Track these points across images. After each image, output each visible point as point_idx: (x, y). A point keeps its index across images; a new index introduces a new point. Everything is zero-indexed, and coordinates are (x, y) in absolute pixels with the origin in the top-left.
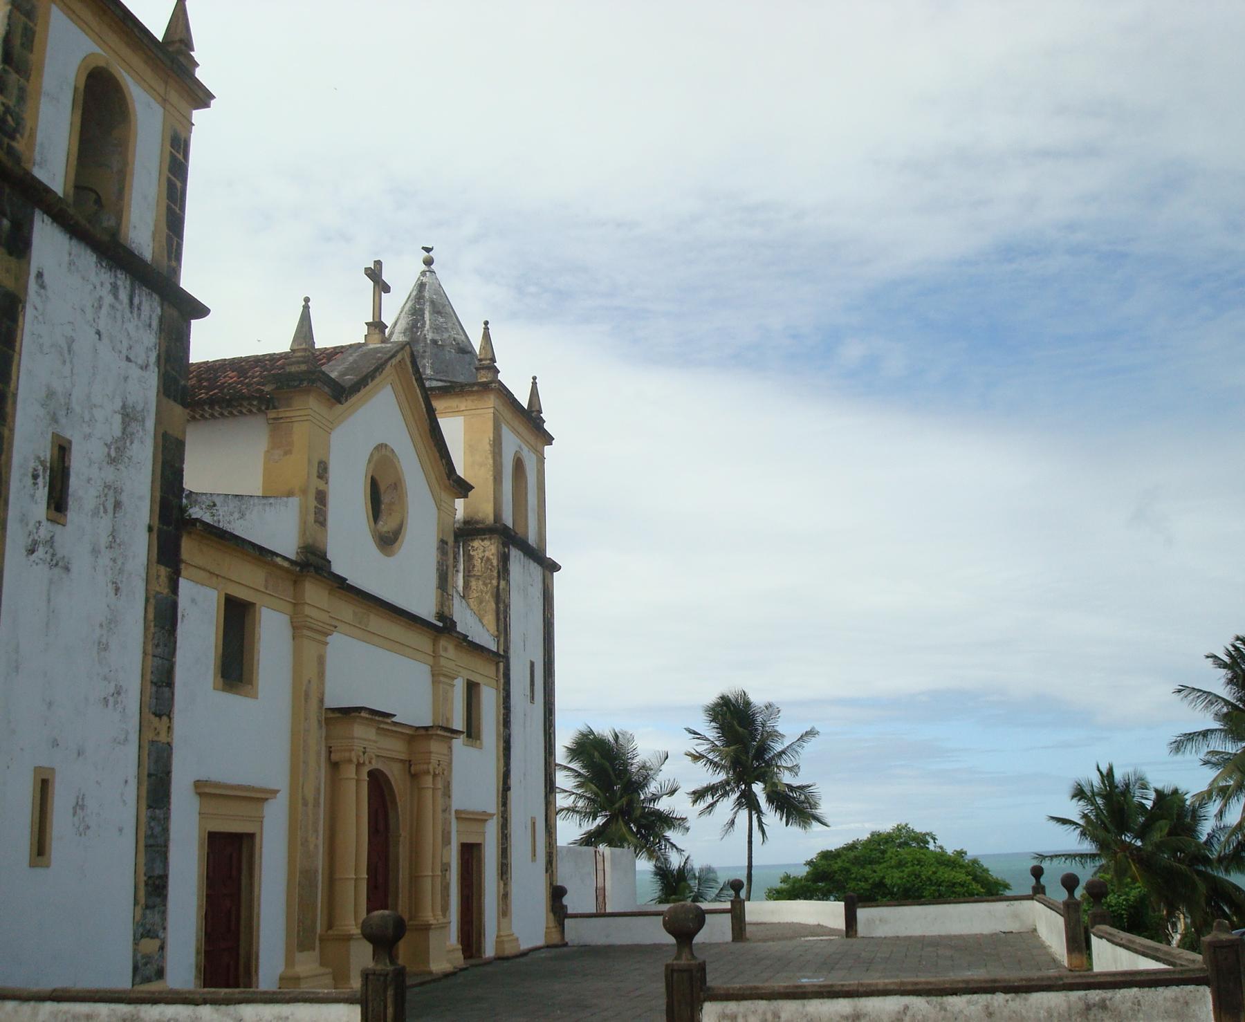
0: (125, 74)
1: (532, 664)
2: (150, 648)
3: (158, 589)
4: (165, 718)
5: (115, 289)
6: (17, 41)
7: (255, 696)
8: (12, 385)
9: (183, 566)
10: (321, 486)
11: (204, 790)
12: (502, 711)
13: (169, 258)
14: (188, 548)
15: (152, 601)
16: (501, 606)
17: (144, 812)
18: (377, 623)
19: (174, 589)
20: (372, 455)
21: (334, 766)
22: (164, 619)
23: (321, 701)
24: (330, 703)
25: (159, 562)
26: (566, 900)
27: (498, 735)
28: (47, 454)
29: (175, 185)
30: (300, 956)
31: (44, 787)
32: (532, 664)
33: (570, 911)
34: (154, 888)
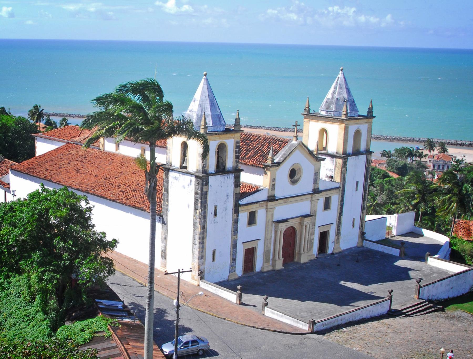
1: (357, 182)
5: (224, 178)
10: (273, 183)
12: (340, 199)
14: (240, 209)
17: (232, 250)
18: (290, 199)
19: (238, 216)
21: (276, 232)
22: (236, 222)
24: (275, 220)
26: (365, 235)
27: (338, 205)
28: (213, 209)
30: (265, 264)
31: (214, 252)
32: (357, 182)
33: (366, 238)
34: (234, 260)
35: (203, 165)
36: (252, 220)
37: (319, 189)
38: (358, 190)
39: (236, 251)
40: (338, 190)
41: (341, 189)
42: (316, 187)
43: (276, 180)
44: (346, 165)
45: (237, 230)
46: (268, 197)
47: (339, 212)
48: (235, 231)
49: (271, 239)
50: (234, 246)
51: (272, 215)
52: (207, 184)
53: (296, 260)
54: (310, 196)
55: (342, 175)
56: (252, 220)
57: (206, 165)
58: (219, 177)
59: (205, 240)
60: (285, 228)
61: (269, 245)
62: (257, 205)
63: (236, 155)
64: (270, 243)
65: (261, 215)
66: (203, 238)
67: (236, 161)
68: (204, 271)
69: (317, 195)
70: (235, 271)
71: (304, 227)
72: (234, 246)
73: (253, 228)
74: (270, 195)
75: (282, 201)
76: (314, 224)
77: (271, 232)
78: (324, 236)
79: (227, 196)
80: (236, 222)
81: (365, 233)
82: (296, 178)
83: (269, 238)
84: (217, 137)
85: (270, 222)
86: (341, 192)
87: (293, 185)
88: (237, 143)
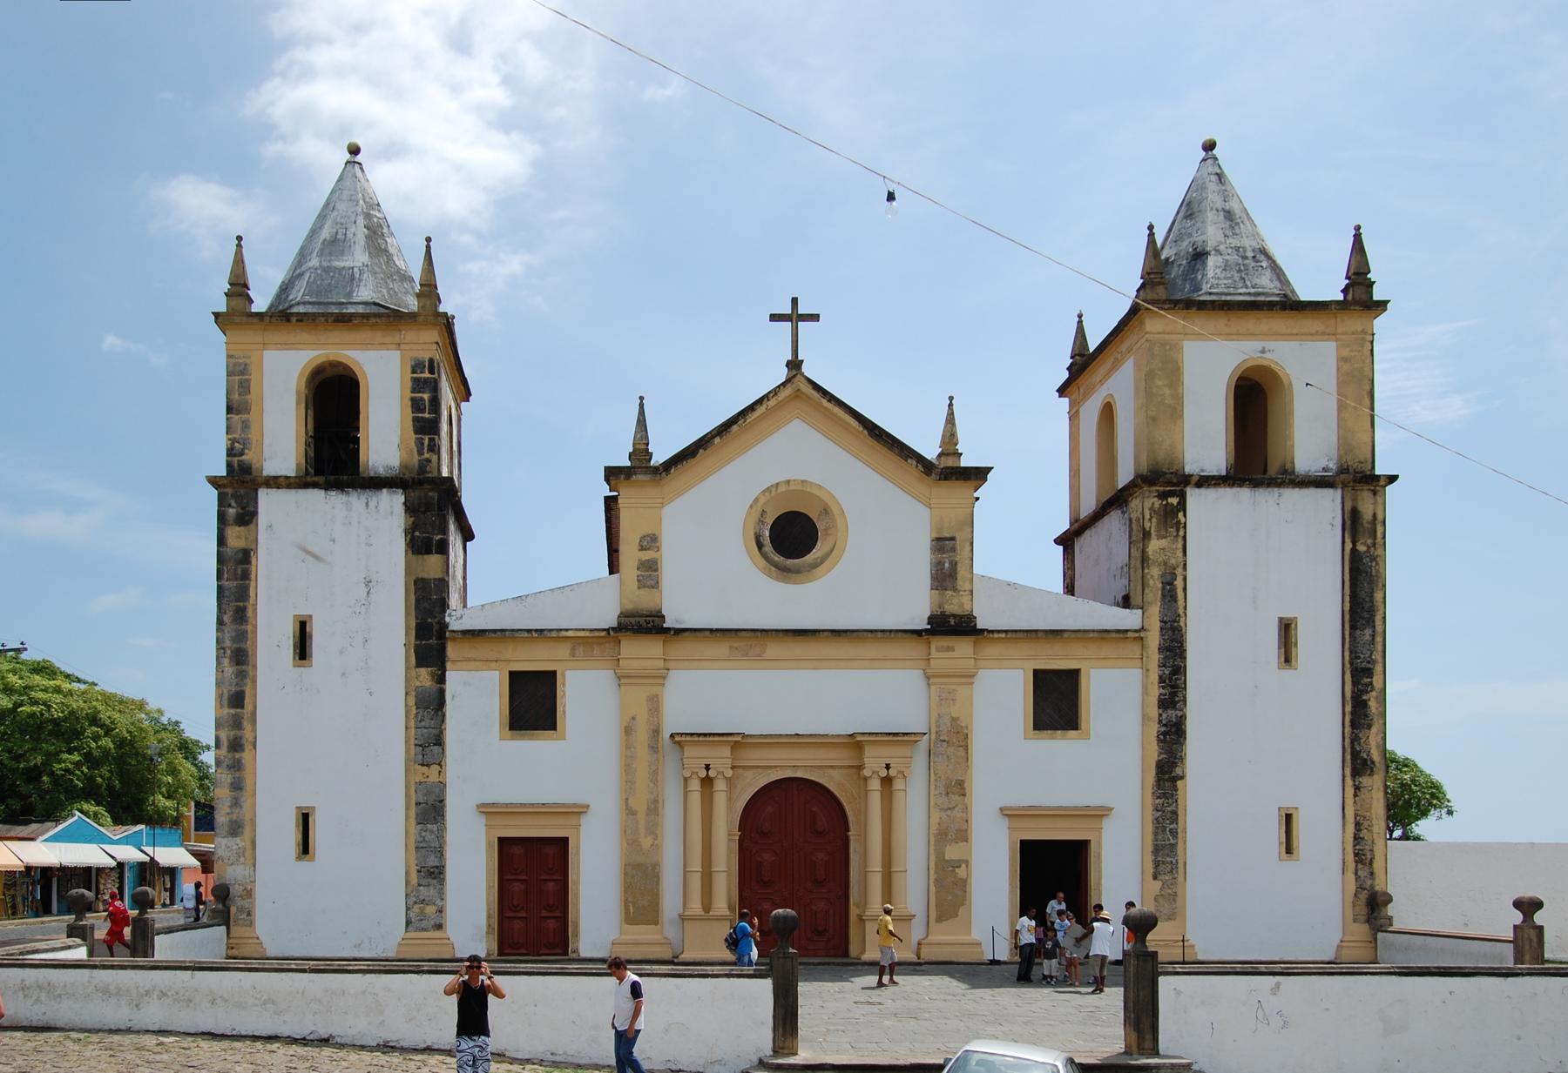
2: (412, 724)
4: (435, 768)
6: (236, 397)
9: (448, 665)
11: (489, 811)
12: (1155, 692)
13: (420, 453)
14: (452, 650)
16: (1155, 572)
18: (774, 649)
19: (441, 679)
20: (756, 500)
23: (656, 732)
25: (419, 664)
26: (1391, 910)
27: (1145, 718)
29: (422, 399)
35: (233, 441)
36: (533, 705)
37: (970, 618)
39: (441, 837)
40: (1134, 649)
41: (1154, 639)
42: (952, 607)
44: (1181, 527)
45: (439, 741)
46: (622, 615)
47: (1154, 753)
49: (654, 809)
50: (429, 810)
51: (655, 705)
52: (247, 517)
53: (854, 950)
54: (914, 649)
55: (1155, 572)
56: (533, 705)
57: (246, 443)
58: (315, 498)
59: (246, 756)
60: (754, 783)
61: (646, 842)
62: (563, 651)
63: (415, 420)
64: (653, 830)
65: (585, 693)
67: (420, 443)
68: (249, 894)
69: (963, 647)
70: (439, 927)
71: (875, 784)
72: (429, 810)
73: (535, 747)
74: (630, 606)
75: (721, 649)
76: (958, 788)
77: (655, 778)
78: (1053, 870)
79: (368, 582)
81: (1389, 899)
83: (640, 803)
84: (304, 336)
85: (642, 734)
86: (1154, 657)
87: (785, 573)
88: (417, 366)
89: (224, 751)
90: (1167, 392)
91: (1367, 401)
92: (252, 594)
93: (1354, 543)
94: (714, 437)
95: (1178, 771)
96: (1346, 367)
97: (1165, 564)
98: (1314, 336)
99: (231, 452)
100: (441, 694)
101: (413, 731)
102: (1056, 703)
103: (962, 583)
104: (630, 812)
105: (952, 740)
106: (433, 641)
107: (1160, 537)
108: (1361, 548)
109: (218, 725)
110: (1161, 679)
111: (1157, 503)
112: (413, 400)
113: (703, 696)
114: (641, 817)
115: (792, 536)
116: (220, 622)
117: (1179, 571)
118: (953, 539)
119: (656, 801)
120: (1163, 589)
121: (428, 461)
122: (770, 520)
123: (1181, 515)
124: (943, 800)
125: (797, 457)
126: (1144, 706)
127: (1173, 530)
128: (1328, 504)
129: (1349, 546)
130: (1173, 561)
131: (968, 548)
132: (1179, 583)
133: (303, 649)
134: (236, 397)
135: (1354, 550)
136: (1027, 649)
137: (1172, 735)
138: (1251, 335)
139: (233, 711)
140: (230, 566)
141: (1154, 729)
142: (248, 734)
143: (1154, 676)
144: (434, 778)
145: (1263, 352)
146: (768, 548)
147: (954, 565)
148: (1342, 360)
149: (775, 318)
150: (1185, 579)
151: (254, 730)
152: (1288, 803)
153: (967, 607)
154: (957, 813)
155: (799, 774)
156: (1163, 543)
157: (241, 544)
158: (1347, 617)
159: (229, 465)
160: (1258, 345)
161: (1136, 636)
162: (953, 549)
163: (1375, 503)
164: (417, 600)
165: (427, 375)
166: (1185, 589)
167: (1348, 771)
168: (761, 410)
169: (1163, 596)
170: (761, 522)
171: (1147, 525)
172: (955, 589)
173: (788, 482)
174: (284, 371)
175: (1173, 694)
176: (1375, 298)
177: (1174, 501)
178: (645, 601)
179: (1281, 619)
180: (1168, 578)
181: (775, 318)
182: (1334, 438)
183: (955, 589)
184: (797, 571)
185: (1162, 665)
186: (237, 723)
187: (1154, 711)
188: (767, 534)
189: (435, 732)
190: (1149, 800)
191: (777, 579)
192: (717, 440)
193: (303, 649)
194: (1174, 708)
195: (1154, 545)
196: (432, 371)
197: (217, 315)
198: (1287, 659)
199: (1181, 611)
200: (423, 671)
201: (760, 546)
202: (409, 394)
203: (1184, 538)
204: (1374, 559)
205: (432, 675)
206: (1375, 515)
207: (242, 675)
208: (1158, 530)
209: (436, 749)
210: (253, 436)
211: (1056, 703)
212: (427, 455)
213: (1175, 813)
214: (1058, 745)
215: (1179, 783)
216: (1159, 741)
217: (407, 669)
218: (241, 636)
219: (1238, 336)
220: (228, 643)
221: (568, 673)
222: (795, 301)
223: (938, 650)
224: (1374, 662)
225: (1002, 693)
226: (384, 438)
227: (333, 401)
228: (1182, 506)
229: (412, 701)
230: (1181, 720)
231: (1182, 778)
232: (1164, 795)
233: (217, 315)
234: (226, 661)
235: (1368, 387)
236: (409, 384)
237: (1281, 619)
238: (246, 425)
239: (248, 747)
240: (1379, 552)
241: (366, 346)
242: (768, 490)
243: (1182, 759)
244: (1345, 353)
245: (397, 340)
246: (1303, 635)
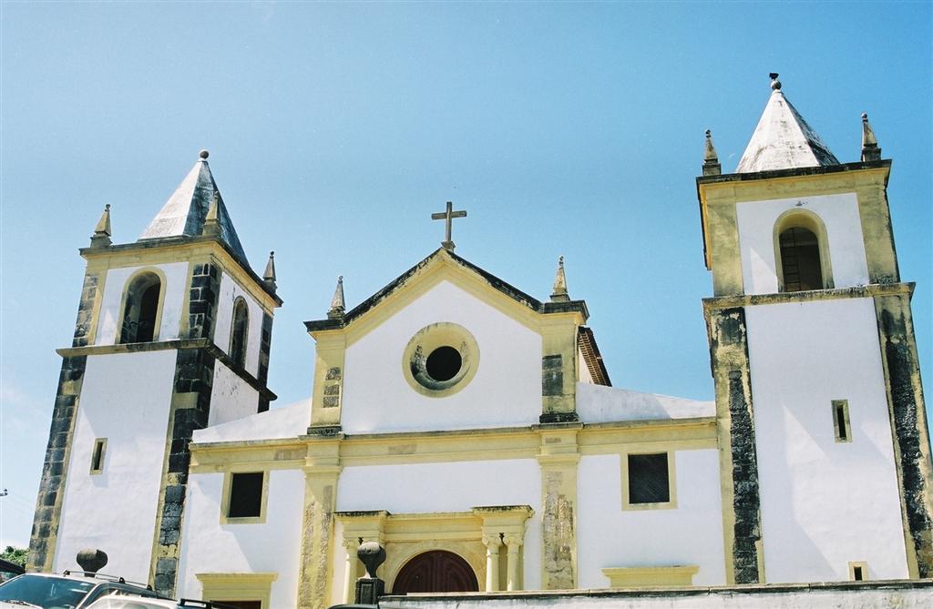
0: (157, 266)
3: (169, 485)
7: (264, 522)
8: (71, 430)
9: (190, 471)
13: (192, 325)
15: (165, 491)
18: (422, 445)
19: (184, 480)
20: (413, 339)
22: (175, 500)
27: (724, 489)
28: (91, 449)
29: (198, 290)
35: (80, 327)
36: (245, 497)
38: (852, 428)
41: (727, 423)
43: (347, 373)
45: (177, 527)
47: (732, 518)
48: (170, 530)
51: (329, 494)
56: (245, 497)
57: (86, 329)
63: (191, 304)
66: (45, 532)
67: (192, 318)
69: (567, 435)
74: (317, 421)
77: (327, 548)
80: (175, 500)
82: (459, 375)
83: (313, 571)
86: (728, 438)
89: (37, 534)
90: (726, 239)
91: (887, 232)
92: (72, 424)
93: (888, 338)
94: (380, 296)
95: (755, 533)
96: (867, 209)
97: (732, 365)
98: (839, 189)
99: (77, 334)
100: (184, 489)
101: (161, 518)
102: (648, 479)
103: (567, 389)
104: (305, 578)
105: (563, 511)
106: (183, 453)
107: (725, 344)
108: (895, 341)
109: (36, 518)
110: (735, 456)
111: (722, 319)
112: (192, 291)
113: (366, 484)
114: (313, 582)
115: (441, 366)
116: (50, 446)
117: (744, 370)
118: (559, 356)
119: (325, 569)
120: (731, 384)
121: (197, 330)
122: (426, 353)
123: (741, 326)
124: (553, 565)
125: (447, 307)
126: (723, 479)
127: (736, 339)
128: (863, 314)
129: (884, 340)
130: (738, 362)
131: (571, 362)
132: (744, 379)
133: (97, 463)
134: (86, 299)
135: (889, 343)
136: (620, 434)
137: (747, 504)
138: (787, 194)
139: (47, 507)
140: (62, 407)
141: (731, 497)
142: (53, 524)
143: (729, 451)
144: (171, 555)
145: (799, 204)
146: (424, 374)
147: (560, 376)
148: (862, 204)
149: (435, 217)
150: (749, 375)
151: (58, 520)
152: (843, 444)
153: (571, 408)
154: (563, 574)
155: (439, 547)
156: (729, 348)
157: (70, 392)
158: (890, 396)
159: (75, 344)
160: (796, 200)
161: (715, 423)
162: (560, 364)
163: (901, 306)
164: (176, 425)
165: (203, 275)
166: (749, 383)
167: (907, 526)
168: (415, 276)
169: (732, 389)
170: (418, 354)
171: (714, 336)
172: (561, 395)
173: (436, 324)
174: (119, 279)
175: (746, 468)
176: (882, 159)
177: (735, 316)
178: (329, 415)
179: (833, 402)
180: (735, 375)
181: (435, 217)
182: (864, 260)
183: (561, 395)
184: (442, 388)
185: (734, 444)
186: (48, 517)
187: (731, 483)
188: (424, 364)
189: (177, 520)
190: (731, 559)
191: (426, 394)
192: (383, 298)
193: (97, 463)
194: (747, 479)
195: (721, 351)
196: (206, 273)
197: (82, 250)
198: (843, 434)
199: (747, 401)
200: (173, 475)
201: (415, 370)
202: (190, 288)
203: (746, 343)
204: (907, 348)
205: (179, 478)
206: (902, 314)
207: (56, 482)
208: (724, 339)
209: (175, 533)
210: (92, 322)
211: (648, 479)
212: (196, 327)
213: (755, 570)
214: (651, 514)
215: (757, 543)
216: (736, 508)
217: (163, 473)
218: (61, 455)
219: (777, 195)
220: (52, 461)
221: (272, 473)
222: (449, 205)
223: (548, 441)
224: (918, 433)
225: (604, 473)
226: (172, 317)
227: (145, 296)
228: (743, 319)
229: (163, 496)
230: (755, 489)
231: (758, 538)
232: (744, 555)
233: (82, 250)
234: (48, 473)
235: (886, 222)
236: (191, 282)
237: (833, 402)
238: (89, 317)
239: (52, 533)
240: (910, 343)
241: (167, 260)
242: (422, 331)
243: (757, 522)
244: (865, 199)
245: (188, 254)
246: (852, 413)
